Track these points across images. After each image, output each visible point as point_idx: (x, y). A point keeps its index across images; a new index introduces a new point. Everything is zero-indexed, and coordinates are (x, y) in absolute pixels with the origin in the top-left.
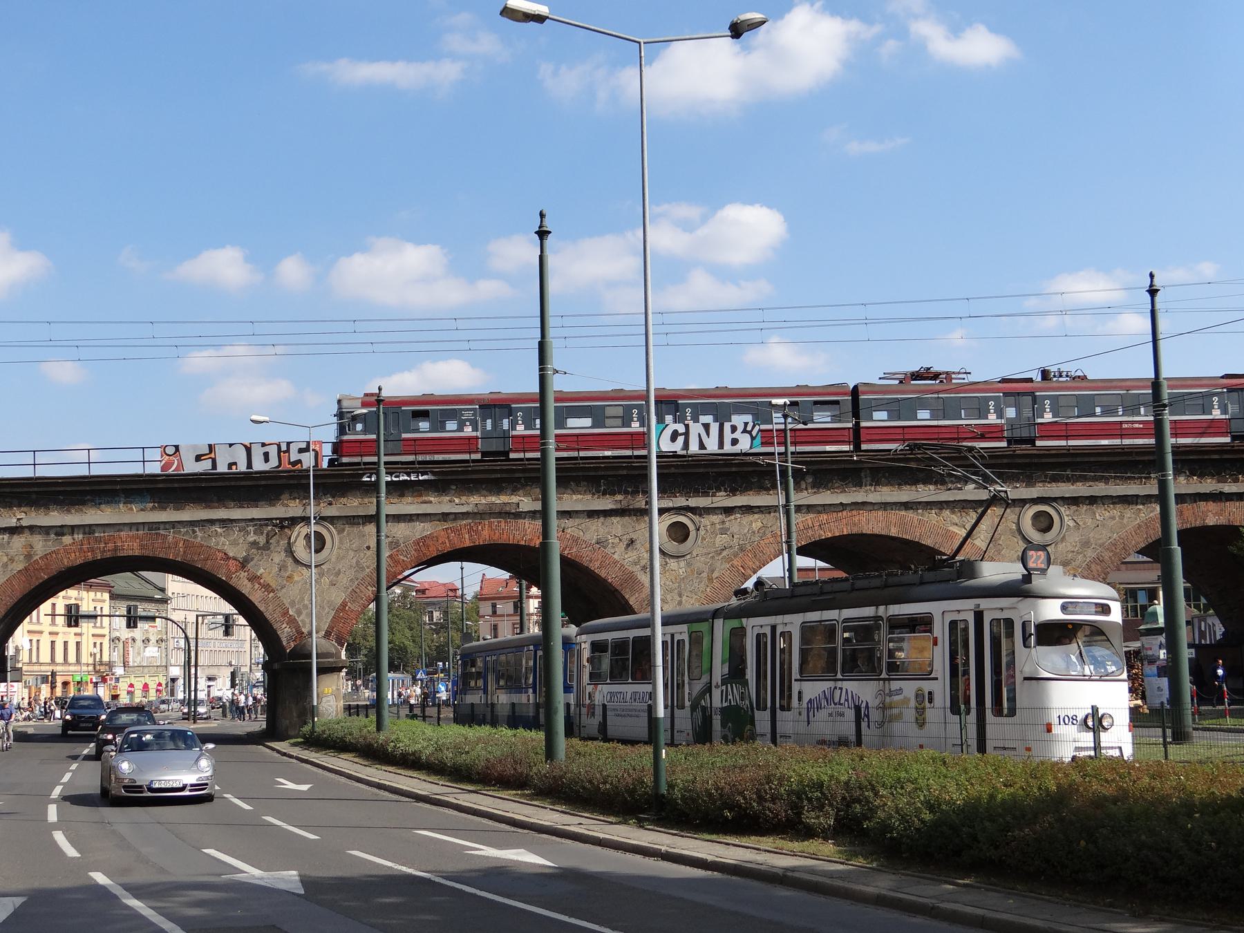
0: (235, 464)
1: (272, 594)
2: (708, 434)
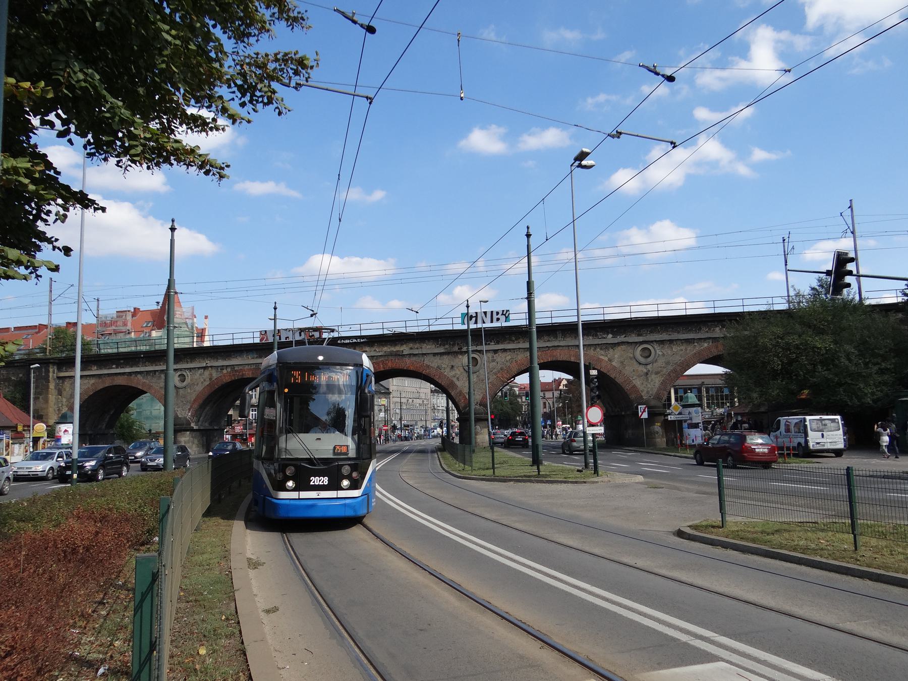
0: (288, 337)
2: (486, 317)
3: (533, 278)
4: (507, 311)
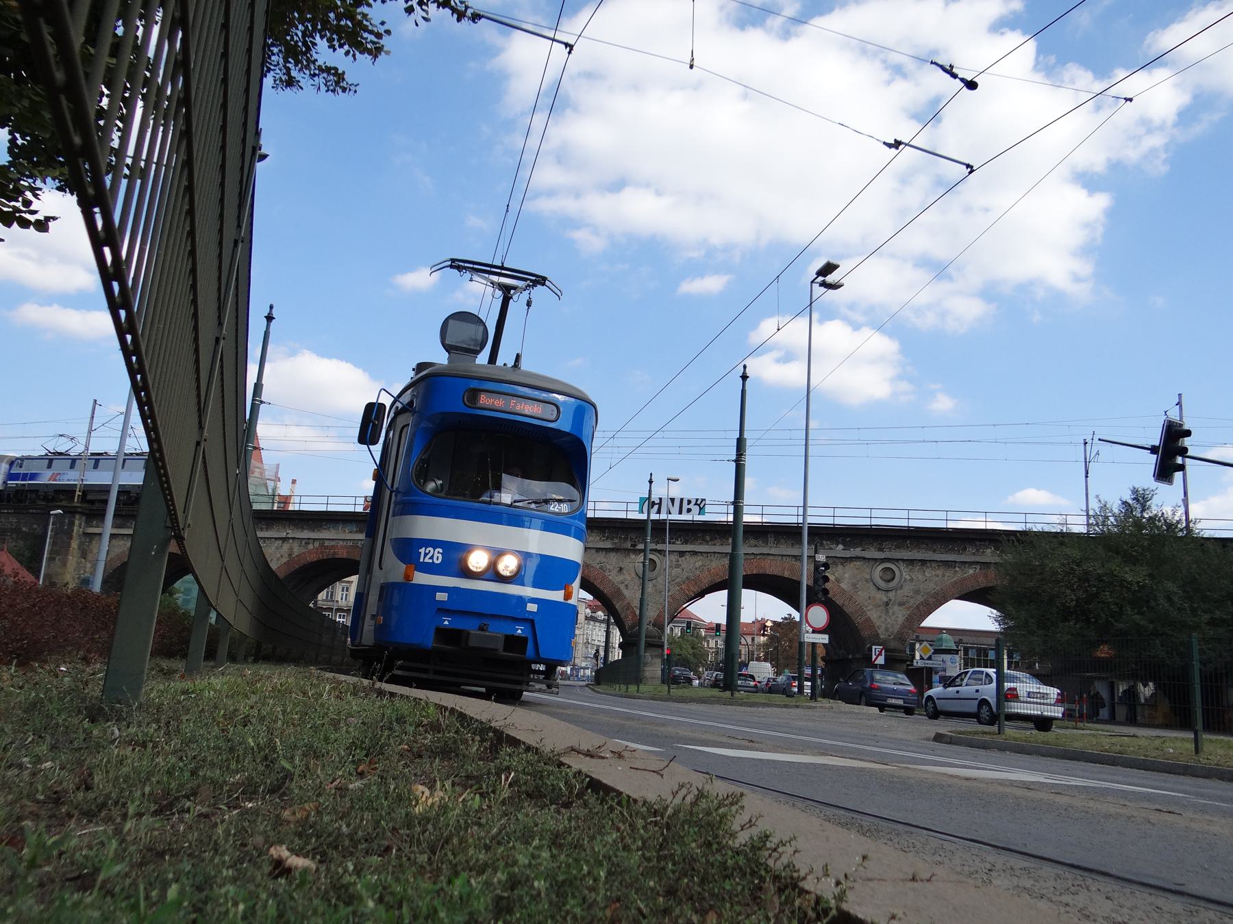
3: (746, 435)
4: (703, 500)
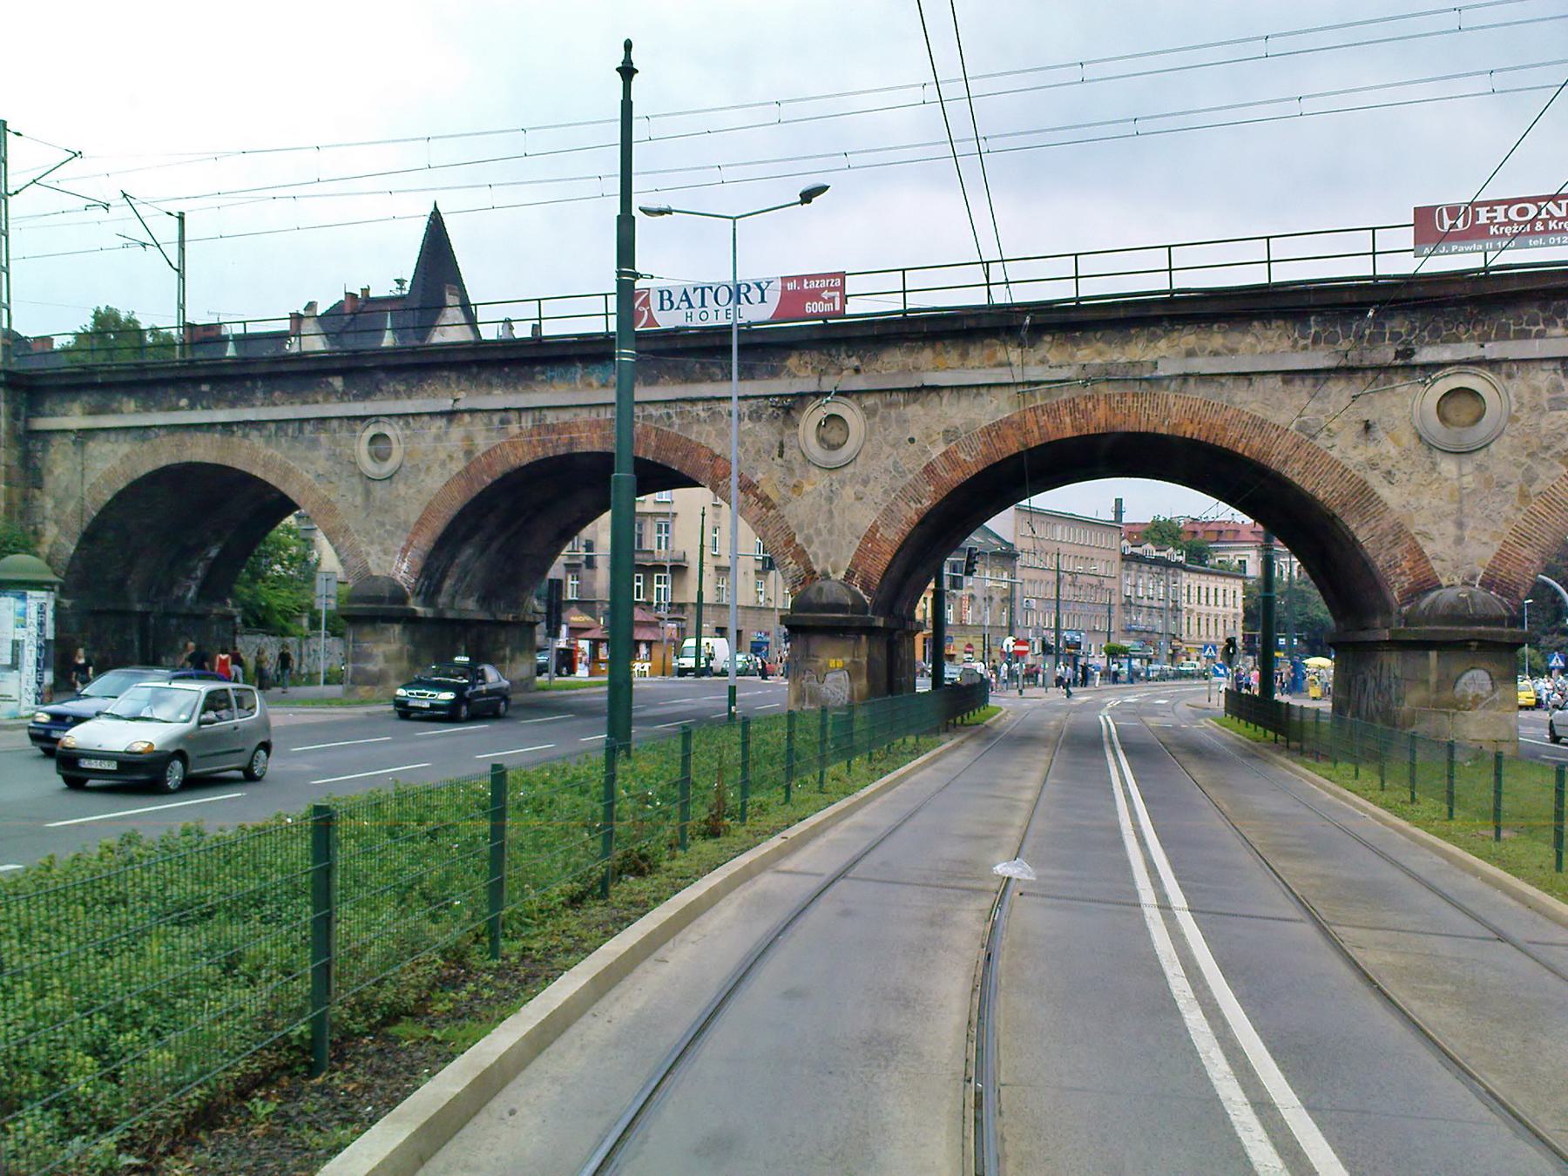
1: (772, 512)
